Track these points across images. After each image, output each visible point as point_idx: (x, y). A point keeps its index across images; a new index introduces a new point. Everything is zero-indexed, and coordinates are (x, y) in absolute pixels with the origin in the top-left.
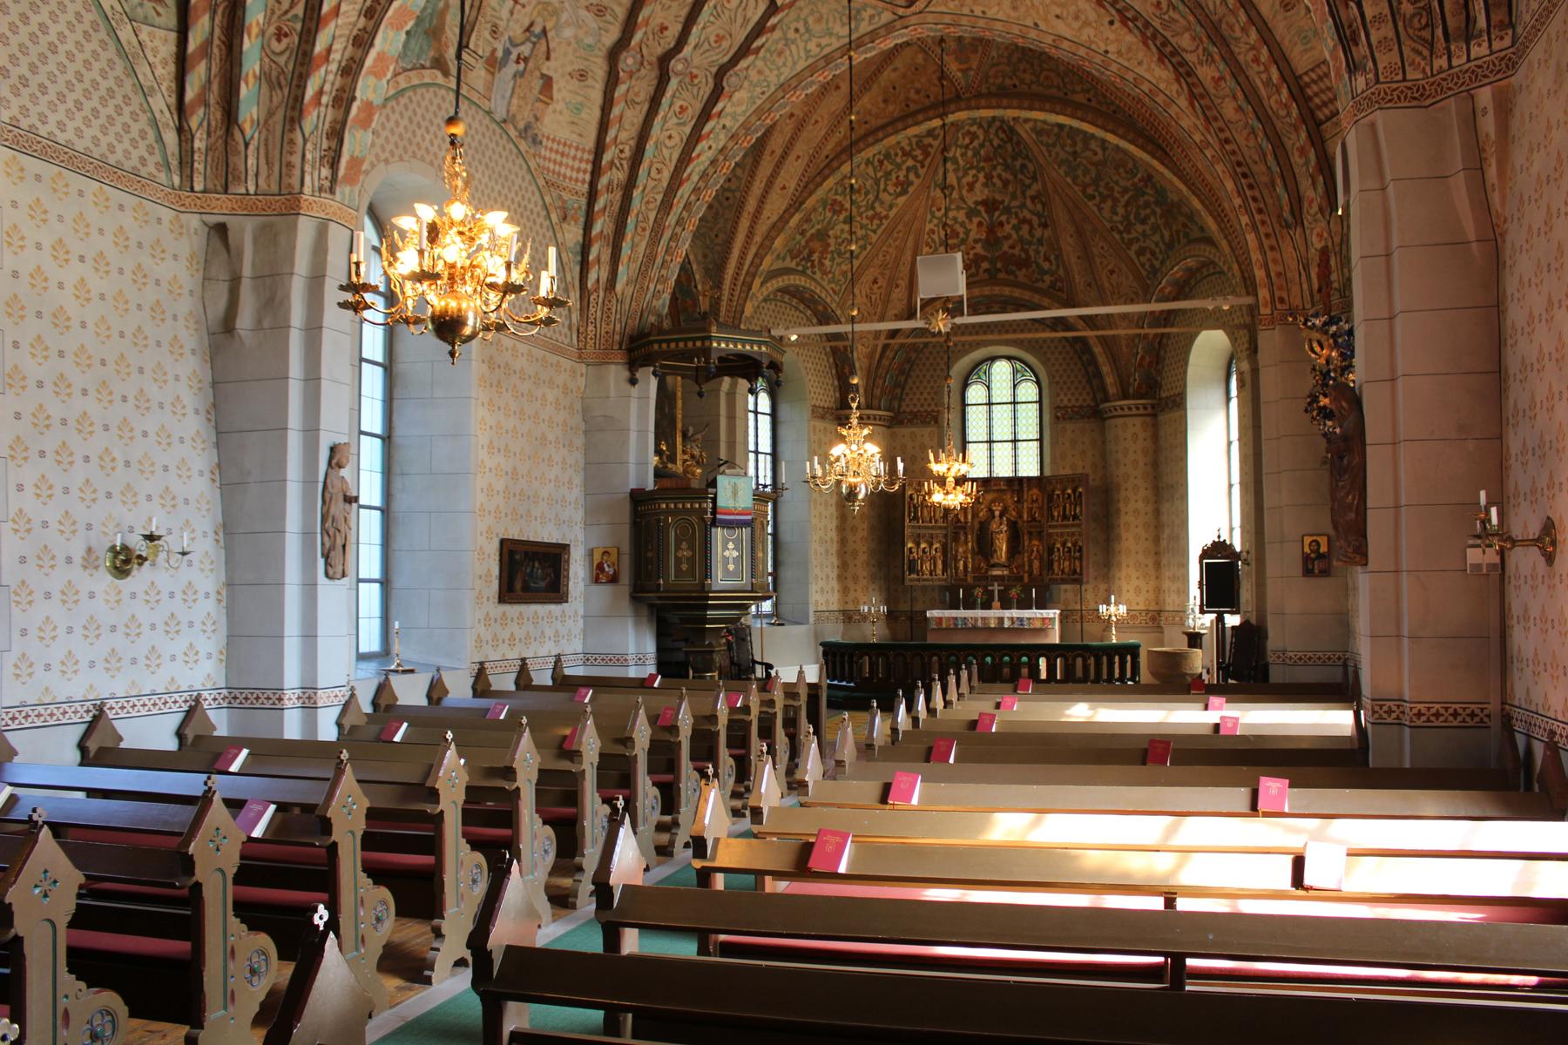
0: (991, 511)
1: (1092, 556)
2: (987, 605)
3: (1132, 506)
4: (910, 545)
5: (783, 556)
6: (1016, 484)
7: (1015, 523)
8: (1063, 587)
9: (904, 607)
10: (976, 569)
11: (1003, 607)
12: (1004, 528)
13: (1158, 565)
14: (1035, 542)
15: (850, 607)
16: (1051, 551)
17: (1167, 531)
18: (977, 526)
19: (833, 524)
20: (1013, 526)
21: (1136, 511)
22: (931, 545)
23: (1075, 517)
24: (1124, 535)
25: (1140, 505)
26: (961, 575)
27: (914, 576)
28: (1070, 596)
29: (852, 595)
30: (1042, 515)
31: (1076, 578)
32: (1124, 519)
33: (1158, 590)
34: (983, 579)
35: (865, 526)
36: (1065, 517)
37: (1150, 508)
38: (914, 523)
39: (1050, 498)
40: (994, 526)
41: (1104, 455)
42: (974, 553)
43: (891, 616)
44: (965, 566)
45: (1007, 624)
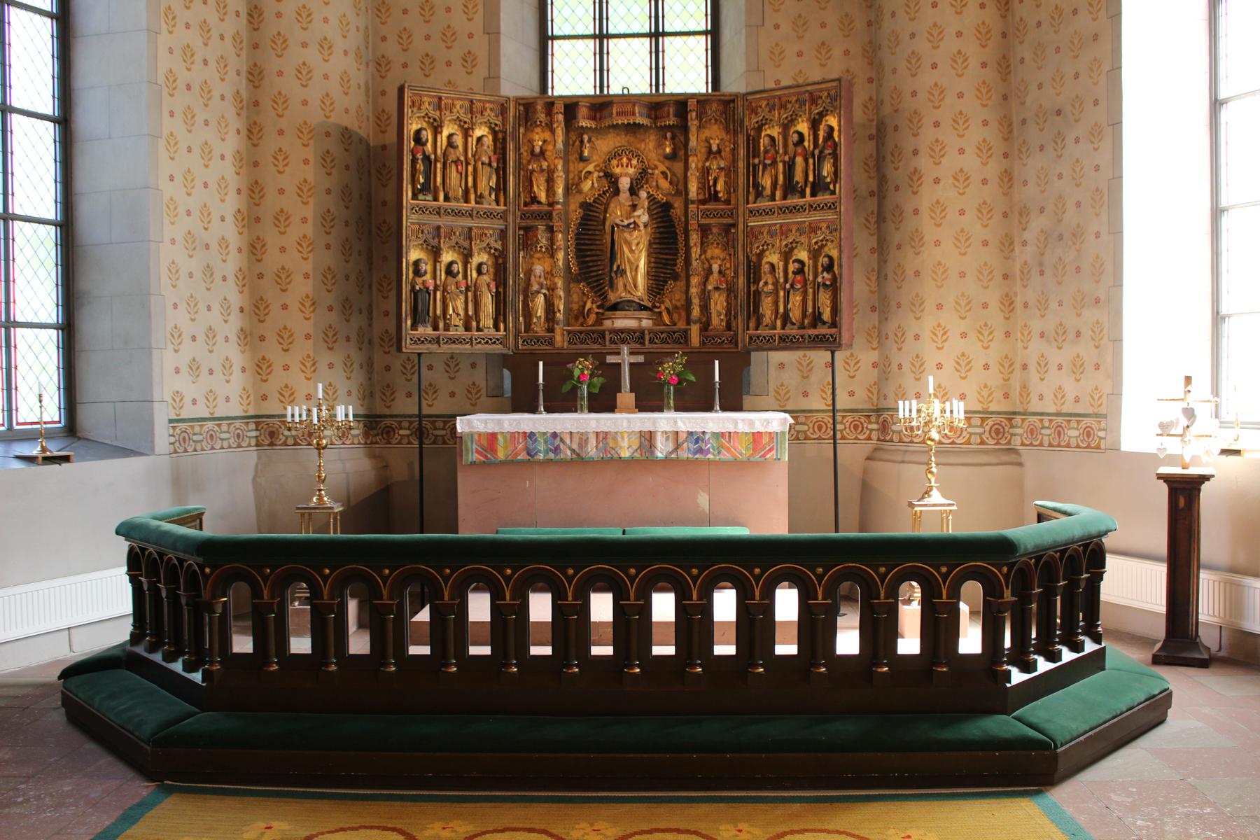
0: (611, 180)
1: (857, 288)
2: (604, 402)
3: (951, 162)
4: (414, 254)
5: (88, 281)
6: (668, 114)
7: (667, 206)
8: (776, 357)
9: (405, 406)
10: (579, 314)
11: (642, 406)
12: (643, 216)
13: (1008, 303)
14: (715, 251)
15: (272, 407)
16: (753, 272)
17: (1038, 223)
18: (576, 215)
19: (230, 204)
20: (661, 212)
21: (961, 177)
22: (467, 256)
23: (818, 186)
24: (930, 232)
25: (970, 161)
26: (539, 328)
27: (425, 330)
28: (791, 378)
29: (277, 379)
30: (731, 187)
31: (821, 332)
32: (927, 195)
33: (1007, 364)
34: (597, 341)
35: (309, 211)
36: (790, 188)
37: (993, 169)
38: (426, 200)
39: (753, 149)
40: (617, 213)
41: (872, 52)
42: (570, 279)
43: (375, 425)
44: (550, 308)
45: (662, 449)
